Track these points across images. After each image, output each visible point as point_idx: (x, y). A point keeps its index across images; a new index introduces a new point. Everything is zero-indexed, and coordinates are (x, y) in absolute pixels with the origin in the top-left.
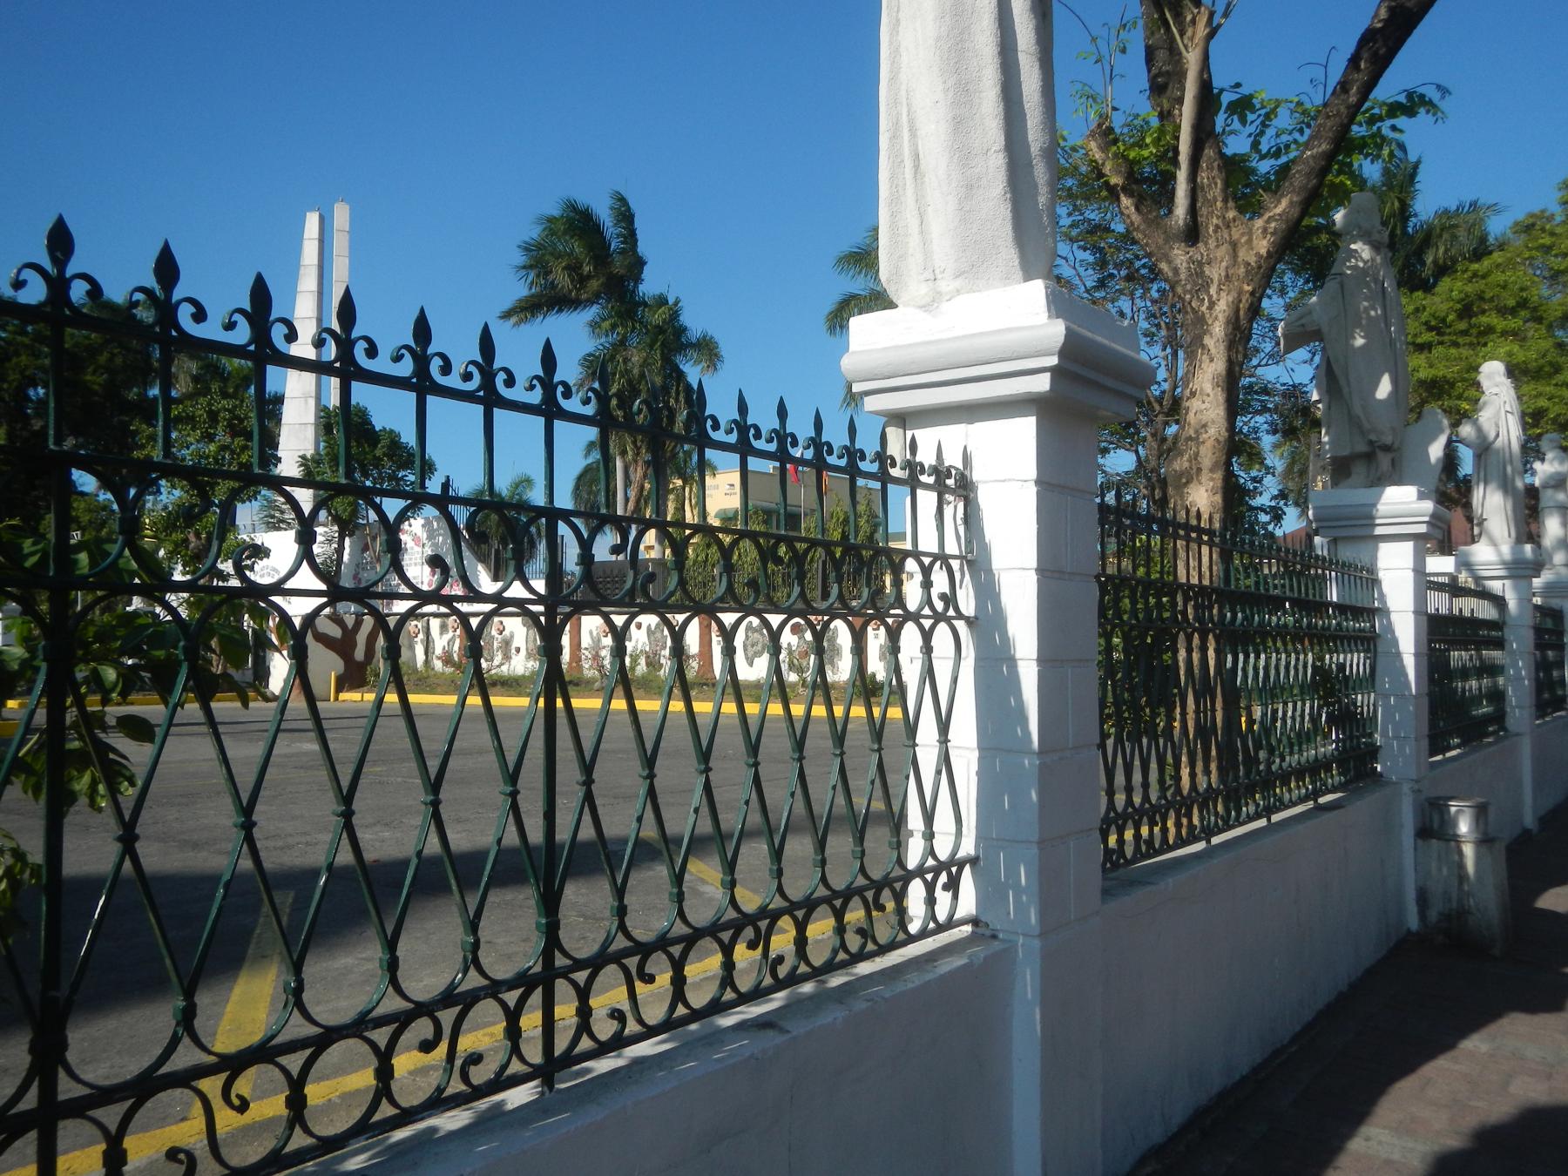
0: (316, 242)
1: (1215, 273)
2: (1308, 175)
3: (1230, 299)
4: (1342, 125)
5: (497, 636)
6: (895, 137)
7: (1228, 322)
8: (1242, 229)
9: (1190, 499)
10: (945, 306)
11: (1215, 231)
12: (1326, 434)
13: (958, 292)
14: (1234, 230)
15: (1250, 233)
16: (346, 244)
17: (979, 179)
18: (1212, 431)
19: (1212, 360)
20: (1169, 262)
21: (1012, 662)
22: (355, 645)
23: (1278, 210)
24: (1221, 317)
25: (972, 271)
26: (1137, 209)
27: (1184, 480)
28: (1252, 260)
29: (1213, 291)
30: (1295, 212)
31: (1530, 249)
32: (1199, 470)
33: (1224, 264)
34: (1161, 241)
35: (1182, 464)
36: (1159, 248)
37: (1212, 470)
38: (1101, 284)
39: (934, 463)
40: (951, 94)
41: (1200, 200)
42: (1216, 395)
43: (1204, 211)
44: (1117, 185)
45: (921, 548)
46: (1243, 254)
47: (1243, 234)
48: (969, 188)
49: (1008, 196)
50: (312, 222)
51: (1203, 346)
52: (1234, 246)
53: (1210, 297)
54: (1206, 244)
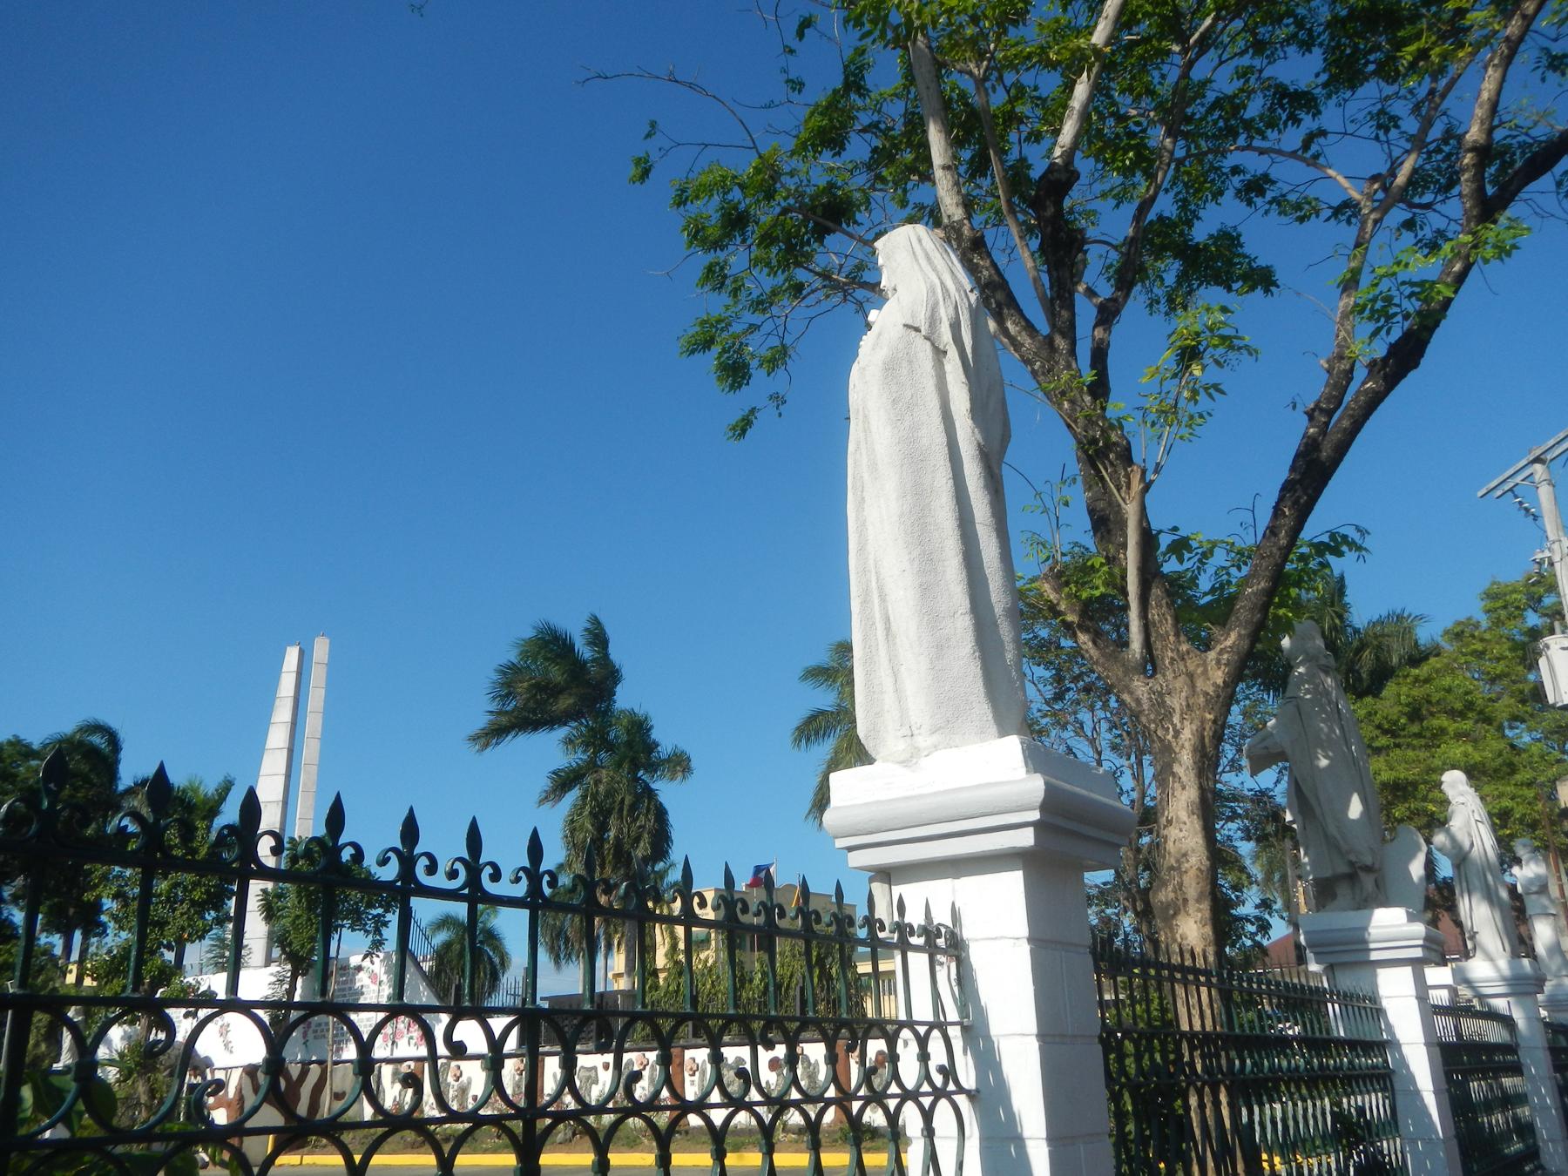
0: (294, 675)
1: (1176, 702)
2: (1251, 610)
3: (1194, 728)
4: (1276, 565)
5: (453, 1083)
6: (866, 602)
7: (1195, 750)
8: (1197, 661)
9: (1180, 931)
10: (924, 762)
11: (1171, 663)
12: (1305, 854)
13: (936, 747)
14: (1189, 662)
15: (1205, 664)
17: (948, 639)
18: (1193, 860)
19: (1184, 788)
20: (1131, 693)
21: (1019, 1141)
22: (297, 1098)
23: (1229, 643)
24: (1187, 745)
25: (947, 726)
26: (1094, 643)
27: (1171, 912)
28: (1211, 690)
29: (1176, 720)
30: (1245, 644)
31: (1465, 655)
32: (1185, 901)
33: (1183, 694)
34: (1120, 673)
35: (1167, 896)
36: (1120, 680)
37: (1198, 901)
38: (1059, 697)
39: (923, 923)
40: (917, 562)
41: (1154, 634)
42: (1192, 822)
43: (1158, 645)
44: (1073, 622)
45: (915, 1018)
46: (1200, 684)
47: (1198, 666)
48: (940, 648)
50: (292, 657)
51: (1174, 774)
52: (1191, 676)
53: (1174, 726)
54: (1164, 675)
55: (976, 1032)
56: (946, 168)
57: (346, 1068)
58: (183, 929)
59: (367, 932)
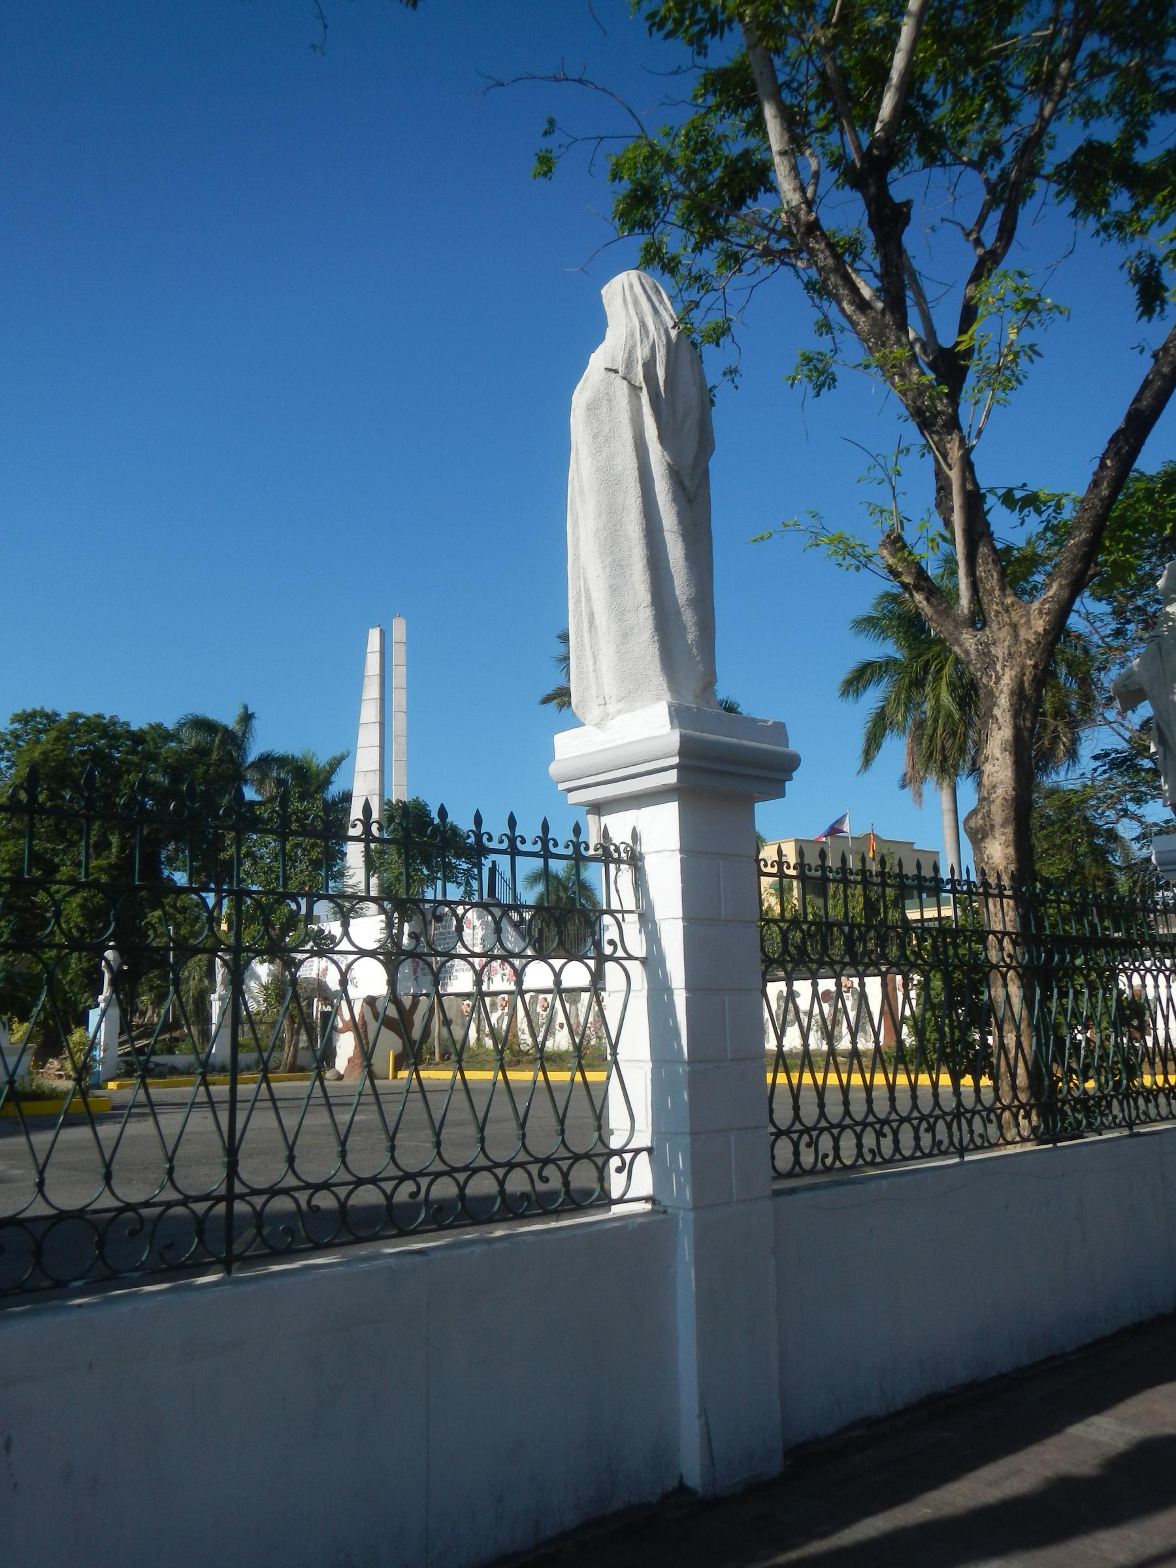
0: (378, 655)
1: (999, 651)
2: (1073, 560)
3: (1014, 673)
4: (1098, 516)
5: (542, 1013)
6: (578, 601)
7: (1012, 694)
8: (1021, 612)
9: (987, 853)
10: (610, 723)
11: (996, 616)
12: (1165, 782)
13: (619, 712)
14: (1013, 613)
15: (1028, 615)
16: (403, 654)
17: (632, 628)
18: (1000, 791)
19: (1000, 729)
20: (960, 645)
21: (670, 991)
22: (412, 1024)
23: (1051, 593)
24: (1005, 690)
25: (631, 696)
26: (927, 599)
27: (980, 836)
28: (1032, 638)
29: (998, 668)
30: (1065, 594)
32: (992, 826)
33: (1006, 643)
34: (951, 628)
35: (976, 822)
36: (951, 634)
37: (1003, 826)
38: (1119, 633)
40: (608, 569)
41: (981, 590)
42: (1004, 758)
43: (985, 600)
44: (909, 584)
46: (1023, 634)
47: (1021, 617)
48: (625, 636)
49: (656, 638)
50: (374, 636)
51: (992, 716)
52: (1014, 627)
53: (997, 673)
54: (990, 627)
55: (646, 918)
56: (783, 153)
57: (450, 1000)
58: (304, 883)
59: (459, 884)
